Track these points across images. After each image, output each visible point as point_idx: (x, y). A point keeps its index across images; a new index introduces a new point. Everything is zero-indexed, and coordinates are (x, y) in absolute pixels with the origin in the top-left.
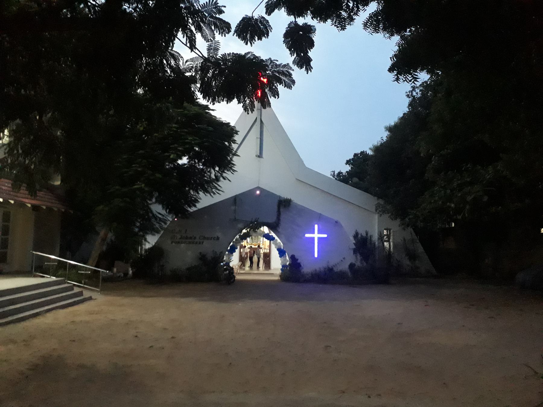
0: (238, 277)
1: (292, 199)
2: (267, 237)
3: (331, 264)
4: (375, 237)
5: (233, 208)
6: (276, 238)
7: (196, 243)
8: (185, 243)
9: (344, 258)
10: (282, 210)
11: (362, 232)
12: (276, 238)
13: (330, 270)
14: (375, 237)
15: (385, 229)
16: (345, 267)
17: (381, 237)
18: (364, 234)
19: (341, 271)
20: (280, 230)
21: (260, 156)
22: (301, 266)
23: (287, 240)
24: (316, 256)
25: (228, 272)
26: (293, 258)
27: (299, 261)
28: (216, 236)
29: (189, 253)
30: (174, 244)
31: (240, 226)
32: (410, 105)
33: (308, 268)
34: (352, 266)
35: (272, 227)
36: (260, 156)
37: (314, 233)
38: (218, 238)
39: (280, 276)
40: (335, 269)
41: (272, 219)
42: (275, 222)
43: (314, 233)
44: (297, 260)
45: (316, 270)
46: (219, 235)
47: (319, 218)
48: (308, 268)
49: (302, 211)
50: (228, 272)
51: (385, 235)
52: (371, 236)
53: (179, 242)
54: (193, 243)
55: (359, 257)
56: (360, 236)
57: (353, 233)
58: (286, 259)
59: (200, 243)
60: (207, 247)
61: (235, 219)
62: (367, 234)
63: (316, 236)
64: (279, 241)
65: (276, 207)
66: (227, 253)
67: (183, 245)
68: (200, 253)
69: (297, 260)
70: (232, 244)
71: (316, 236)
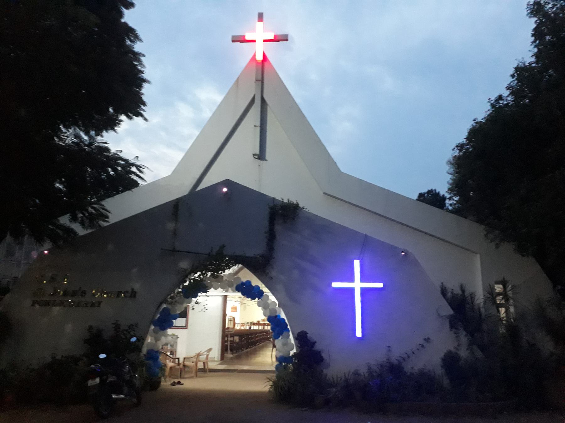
0: (190, 384)
1: (301, 205)
2: (249, 292)
3: (396, 355)
4: (480, 297)
5: (170, 226)
6: (266, 291)
7: (86, 305)
8: (61, 304)
9: (427, 340)
10: (278, 228)
11: (453, 286)
12: (266, 291)
13: (394, 369)
14: (480, 297)
15: (497, 283)
16: (430, 360)
17: (491, 295)
18: (458, 291)
19: (422, 374)
20: (273, 273)
21: (261, 156)
22: (322, 359)
23: (289, 298)
24: (359, 334)
25: (98, 380)
26: (302, 338)
27: (318, 347)
28: (129, 290)
29: (69, 328)
30: (37, 306)
31: (184, 265)
32: (538, 33)
33: (341, 364)
34: (450, 361)
35: (259, 266)
36: (261, 156)
37: (352, 280)
38: (133, 294)
39: (276, 385)
40: (407, 368)
41: (256, 250)
42: (262, 256)
43: (352, 280)
44: (314, 343)
45: (356, 373)
46: (137, 287)
47: (364, 245)
48: (341, 364)
49: (322, 229)
50: (98, 380)
51: (499, 294)
52: (472, 296)
53: (47, 304)
54: (78, 305)
55: (464, 339)
56: (449, 295)
57: (440, 283)
58: (286, 344)
59: (93, 305)
60: (108, 313)
61: (174, 251)
62: (463, 291)
63: (357, 285)
64: (272, 298)
65: (266, 223)
66: (153, 327)
67: (56, 309)
68: (91, 328)
69: (314, 343)
70: (164, 306)
71: (357, 285)
